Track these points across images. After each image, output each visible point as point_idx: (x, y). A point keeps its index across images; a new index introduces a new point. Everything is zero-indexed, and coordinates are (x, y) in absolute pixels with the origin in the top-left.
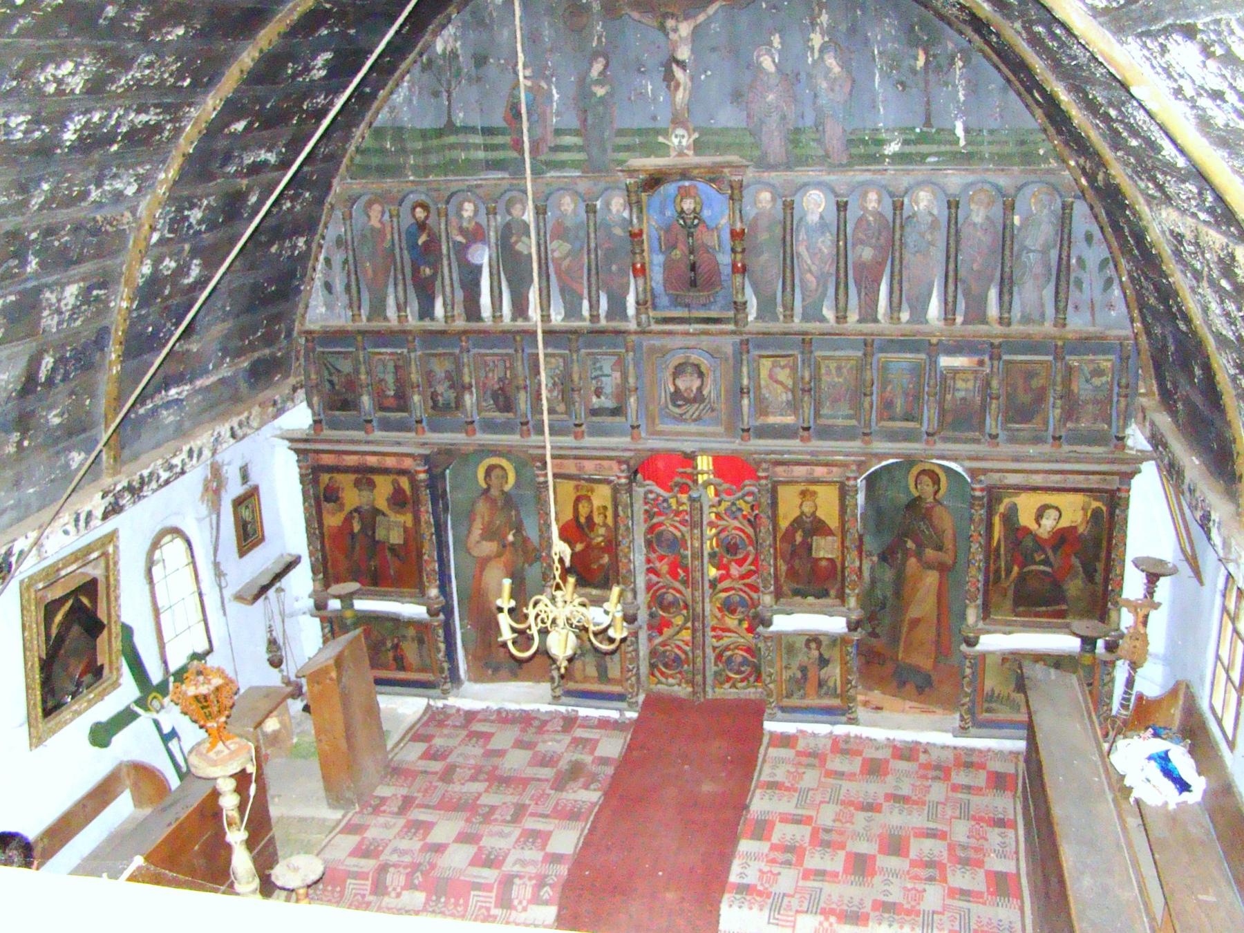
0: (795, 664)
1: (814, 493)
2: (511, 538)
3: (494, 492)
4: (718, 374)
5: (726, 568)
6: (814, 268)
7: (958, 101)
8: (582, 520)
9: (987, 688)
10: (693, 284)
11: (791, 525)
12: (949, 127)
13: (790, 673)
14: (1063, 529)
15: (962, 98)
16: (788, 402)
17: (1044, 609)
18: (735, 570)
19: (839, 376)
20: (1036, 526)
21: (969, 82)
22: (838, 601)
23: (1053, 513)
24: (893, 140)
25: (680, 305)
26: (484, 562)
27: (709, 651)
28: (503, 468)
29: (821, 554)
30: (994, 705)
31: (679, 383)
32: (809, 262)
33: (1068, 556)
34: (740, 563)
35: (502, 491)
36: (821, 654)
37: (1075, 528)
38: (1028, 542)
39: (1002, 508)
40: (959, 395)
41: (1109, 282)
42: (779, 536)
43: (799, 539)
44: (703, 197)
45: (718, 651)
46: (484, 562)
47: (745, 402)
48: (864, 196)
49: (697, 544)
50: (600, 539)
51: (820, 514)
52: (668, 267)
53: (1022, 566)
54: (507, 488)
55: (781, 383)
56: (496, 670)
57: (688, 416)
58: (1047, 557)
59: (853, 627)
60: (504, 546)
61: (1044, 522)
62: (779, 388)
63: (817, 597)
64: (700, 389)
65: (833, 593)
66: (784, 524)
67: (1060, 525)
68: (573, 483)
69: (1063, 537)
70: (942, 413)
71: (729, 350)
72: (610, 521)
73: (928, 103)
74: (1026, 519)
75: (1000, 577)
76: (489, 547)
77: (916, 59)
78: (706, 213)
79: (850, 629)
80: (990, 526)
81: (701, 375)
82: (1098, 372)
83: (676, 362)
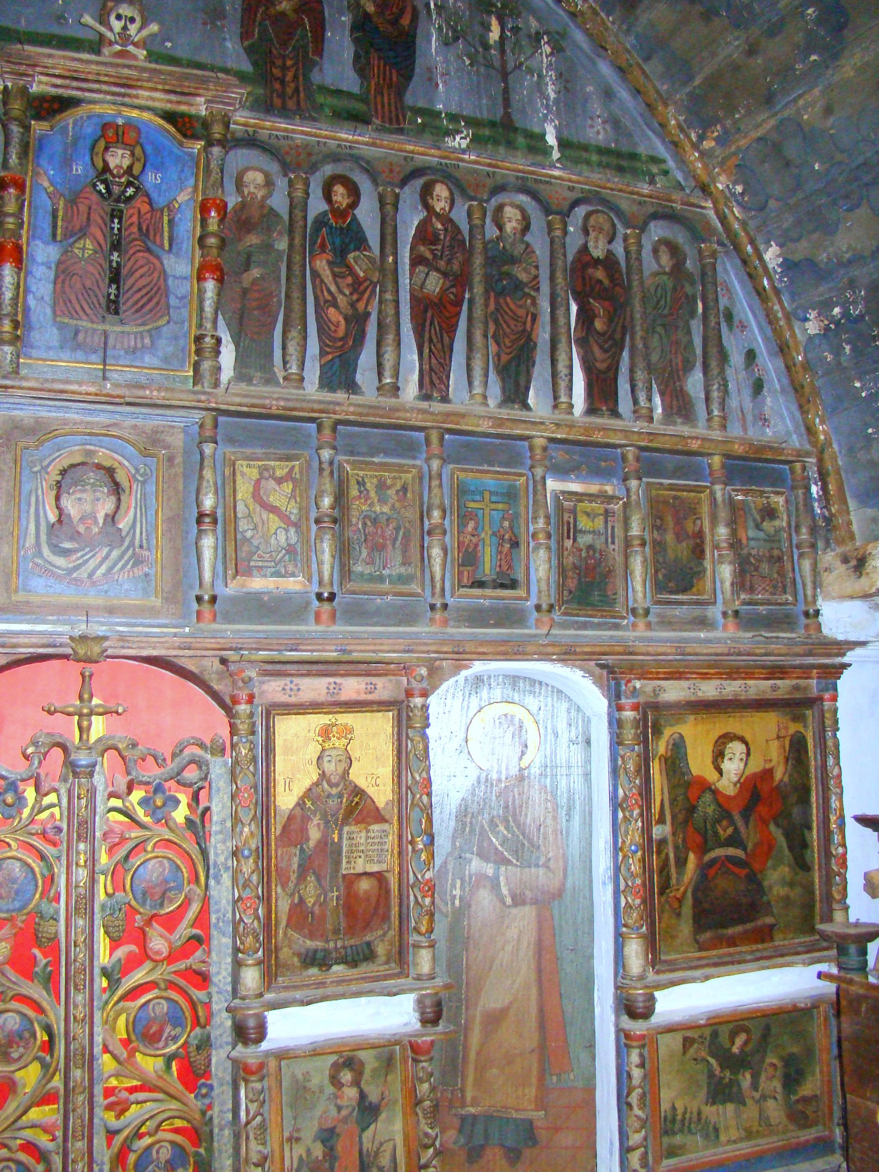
0: (309, 1130)
1: (347, 732)
4: (151, 488)
5: (141, 938)
6: (341, 300)
7: (547, 98)
9: (665, 1106)
10: (113, 307)
11: (301, 804)
12: (537, 130)
13: (299, 1150)
14: (754, 775)
15: (553, 96)
16: (290, 550)
17: (738, 929)
18: (158, 943)
19: (382, 501)
20: (716, 775)
21: (560, 75)
22: (394, 968)
23: (736, 748)
24: (459, 132)
25: (78, 347)
27: (99, 1141)
29: (360, 866)
30: (678, 1139)
31: (67, 503)
32: (333, 288)
33: (766, 823)
34: (170, 922)
36: (362, 1096)
37: (768, 773)
38: (707, 807)
39: (661, 747)
40: (584, 540)
41: (758, 387)
42: (276, 830)
43: (314, 834)
44: (149, 149)
45: (118, 1140)
47: (208, 542)
48: (426, 192)
49: (82, 874)
51: (359, 776)
52: (63, 272)
53: (702, 850)
55: (274, 510)
57: (83, 573)
58: (736, 830)
59: (432, 1014)
61: (726, 765)
62: (274, 521)
63: (353, 963)
64: (112, 518)
65: (381, 949)
66: (286, 800)
67: (747, 773)
69: (756, 789)
70: (562, 571)
71: (177, 440)
73: (506, 91)
74: (699, 764)
75: (668, 878)
77: (487, 28)
78: (151, 179)
79: (424, 1022)
80: (647, 780)
81: (117, 489)
82: (770, 513)
83: (66, 463)
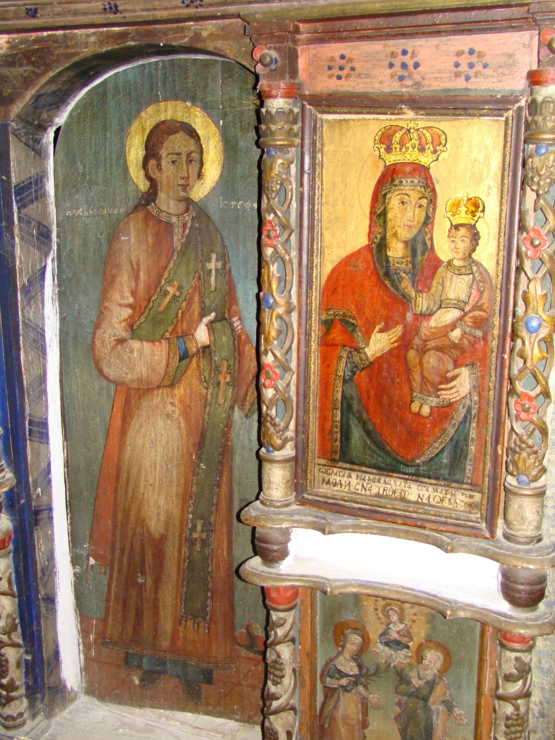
2: (202, 335)
3: (167, 204)
8: (396, 250)
26: (131, 397)
28: (192, 134)
35: (188, 201)
46: (131, 397)
50: (451, 315)
54: (200, 191)
56: (150, 677)
60: (185, 356)
68: (374, 123)
72: (487, 254)
76: (147, 358)
